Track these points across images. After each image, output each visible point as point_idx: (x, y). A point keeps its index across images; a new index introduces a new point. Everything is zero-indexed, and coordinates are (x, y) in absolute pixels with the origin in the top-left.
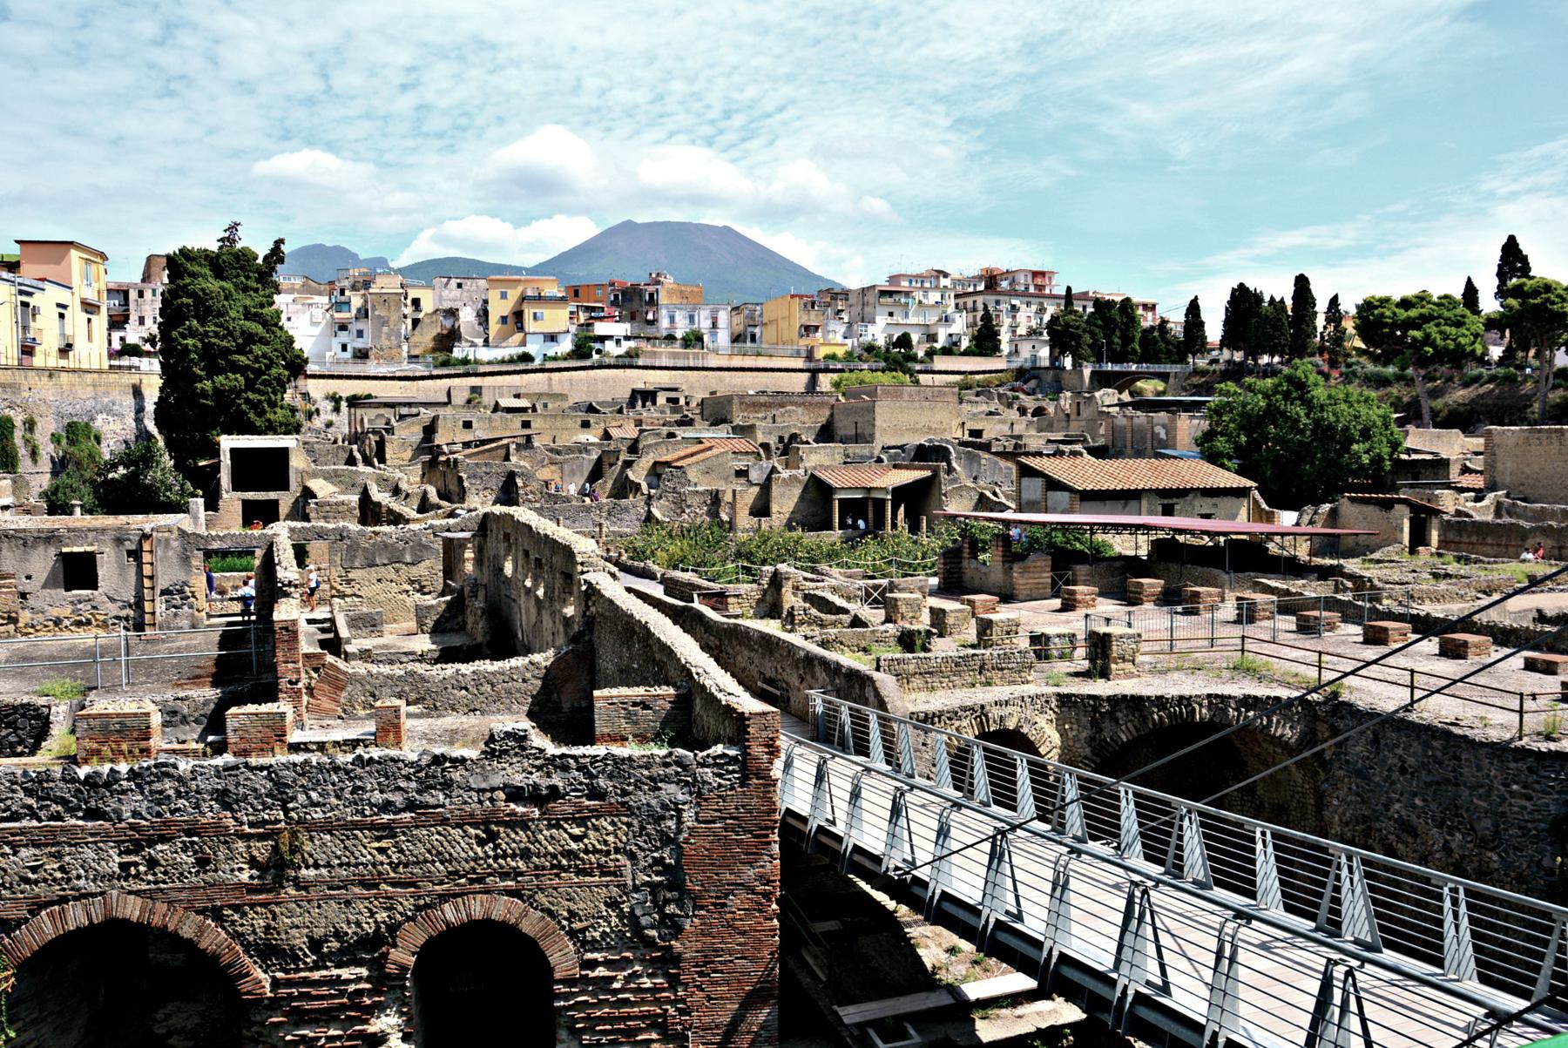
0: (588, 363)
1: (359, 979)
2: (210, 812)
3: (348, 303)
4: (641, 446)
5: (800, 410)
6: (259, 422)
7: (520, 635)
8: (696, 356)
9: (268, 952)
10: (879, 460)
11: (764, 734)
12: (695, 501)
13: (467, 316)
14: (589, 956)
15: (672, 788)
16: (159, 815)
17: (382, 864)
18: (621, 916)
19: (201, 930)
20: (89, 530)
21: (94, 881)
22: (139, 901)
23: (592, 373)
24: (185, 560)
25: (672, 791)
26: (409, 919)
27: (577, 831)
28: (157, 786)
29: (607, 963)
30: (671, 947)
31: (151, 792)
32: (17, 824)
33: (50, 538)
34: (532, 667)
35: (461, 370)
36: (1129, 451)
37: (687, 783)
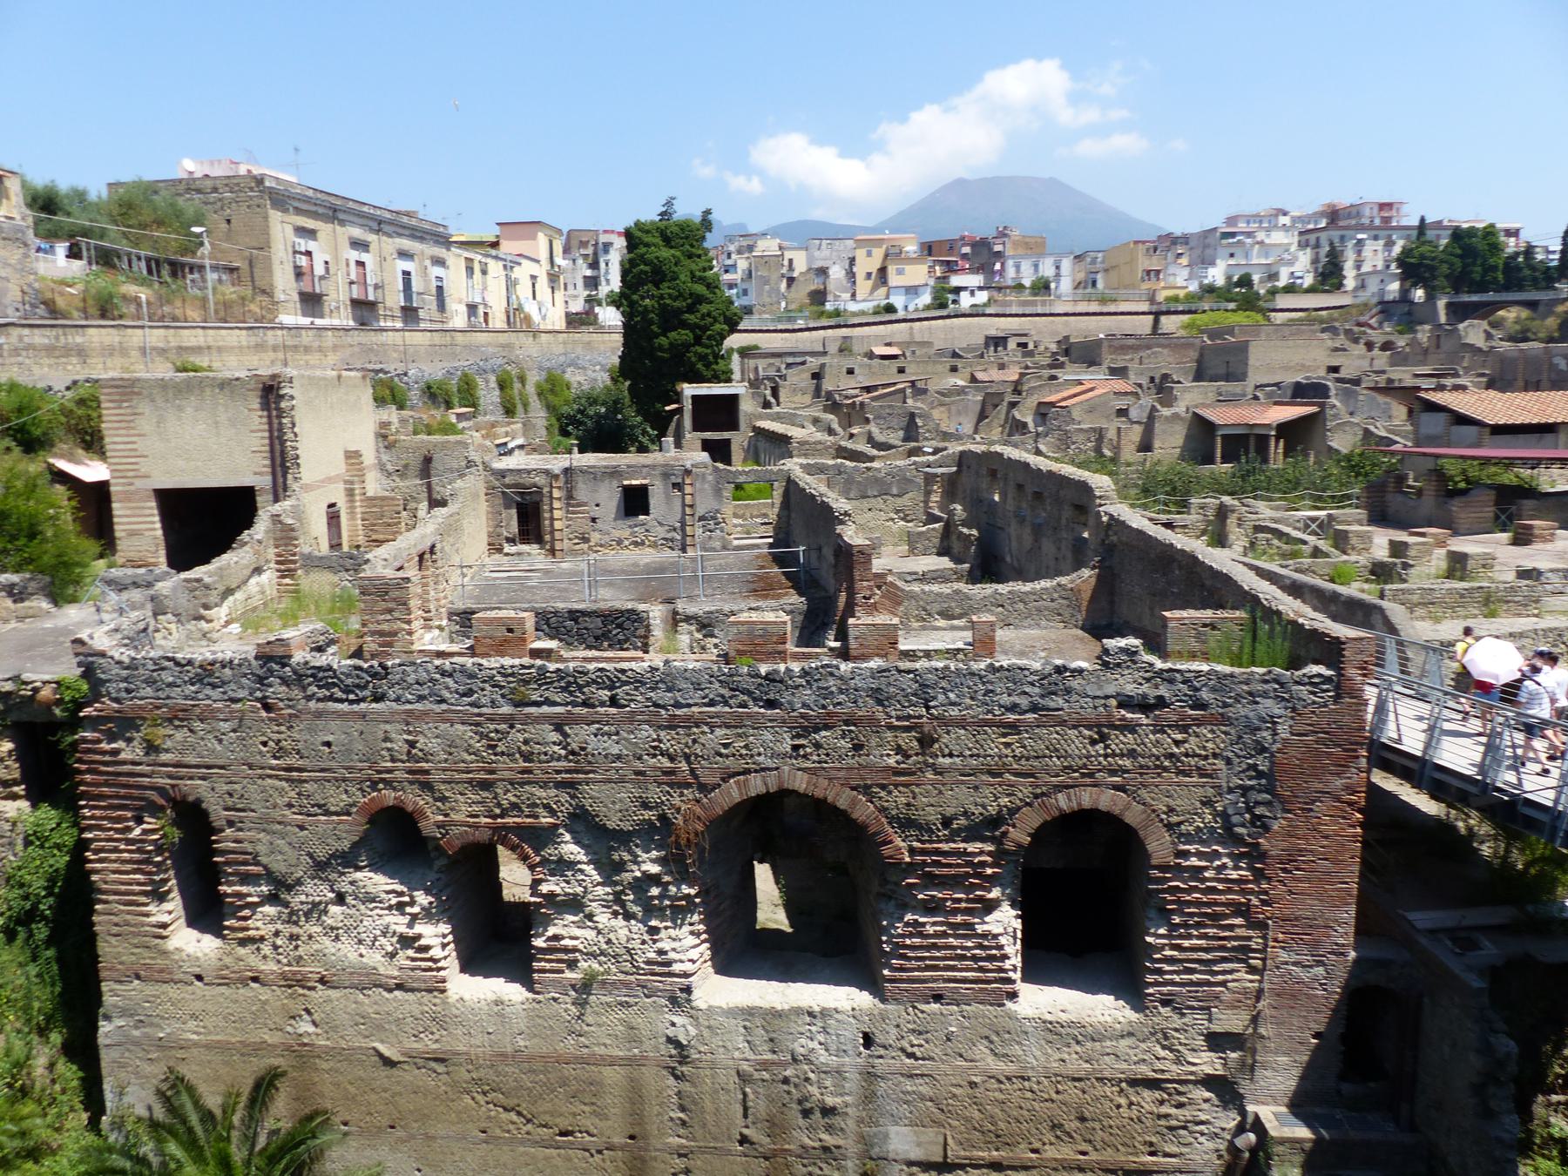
0: (944, 312)
1: (982, 853)
2: (867, 707)
3: (734, 266)
4: (1025, 387)
5: (1165, 351)
6: (708, 374)
7: (1008, 559)
8: (1044, 303)
9: (906, 824)
10: (1256, 398)
11: (1359, 657)
12: (1080, 438)
13: (837, 273)
14: (1182, 847)
15: (1269, 703)
16: (824, 707)
17: (1007, 756)
18: (1215, 814)
19: (854, 802)
20: (644, 466)
21: (771, 757)
22: (806, 776)
23: (948, 321)
24: (718, 492)
25: (1269, 706)
26: (1028, 804)
27: (1179, 737)
28: (823, 684)
29: (1199, 855)
30: (1258, 843)
31: (819, 688)
32: (712, 709)
33: (614, 473)
34: (1059, 589)
35: (832, 322)
36: (1545, 383)
37: (1283, 699)
